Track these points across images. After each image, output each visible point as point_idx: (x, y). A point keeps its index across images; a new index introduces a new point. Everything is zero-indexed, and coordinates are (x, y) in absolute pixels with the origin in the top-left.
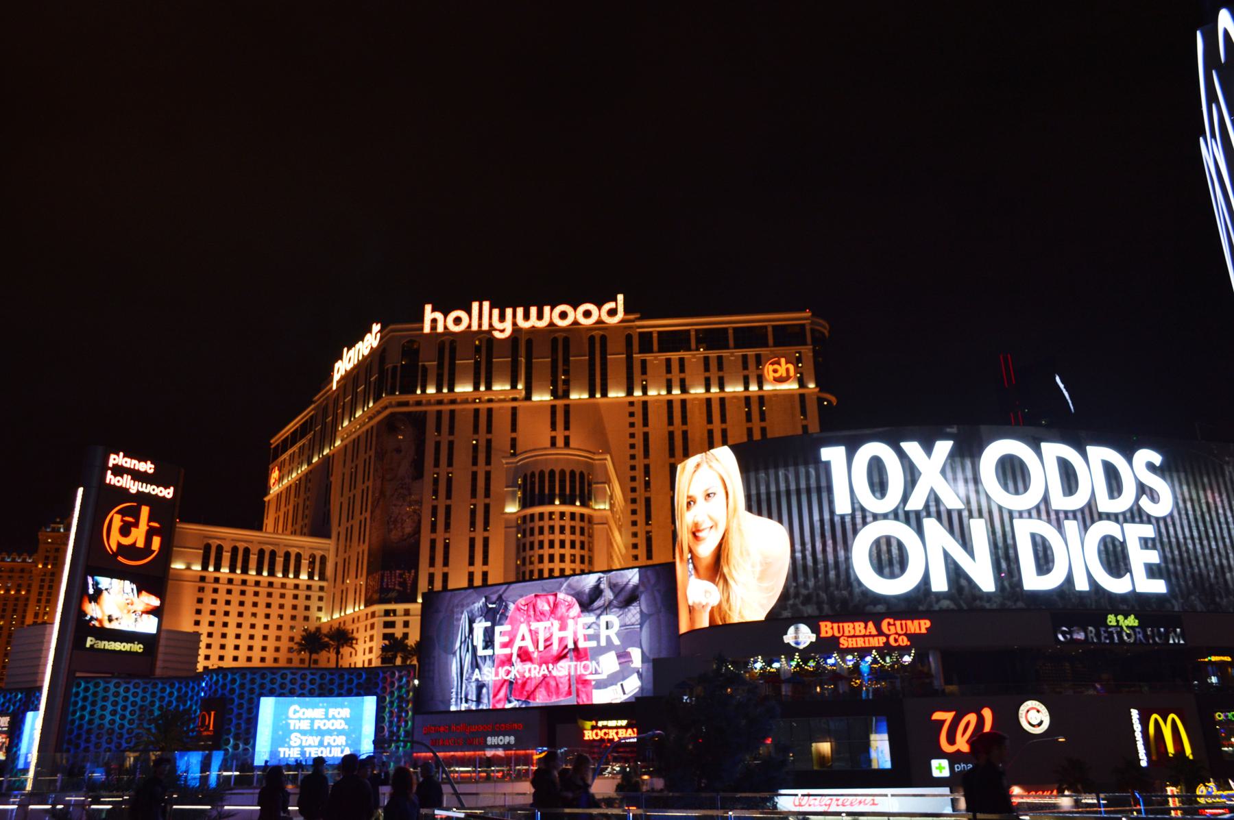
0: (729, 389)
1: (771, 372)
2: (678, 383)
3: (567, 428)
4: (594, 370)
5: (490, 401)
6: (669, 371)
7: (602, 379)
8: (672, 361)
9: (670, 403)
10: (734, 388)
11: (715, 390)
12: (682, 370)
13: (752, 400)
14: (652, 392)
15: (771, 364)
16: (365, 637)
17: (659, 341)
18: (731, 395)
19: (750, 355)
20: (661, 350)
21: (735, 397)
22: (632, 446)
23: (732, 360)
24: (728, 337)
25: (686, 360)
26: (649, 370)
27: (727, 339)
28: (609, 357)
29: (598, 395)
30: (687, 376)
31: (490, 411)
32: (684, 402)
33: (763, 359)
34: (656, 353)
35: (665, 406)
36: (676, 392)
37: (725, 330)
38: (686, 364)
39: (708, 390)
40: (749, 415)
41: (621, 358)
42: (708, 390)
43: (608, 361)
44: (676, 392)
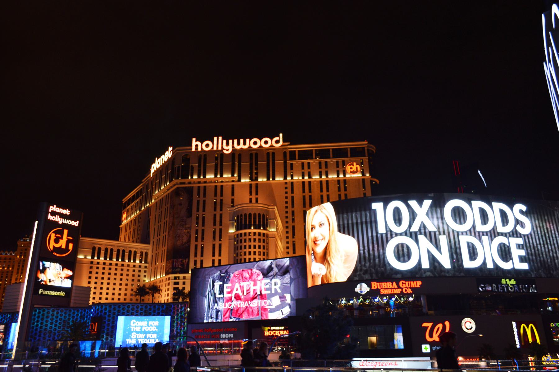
0: (330, 176)
1: (349, 169)
2: (307, 174)
3: (257, 194)
4: (269, 168)
5: (222, 182)
6: (303, 168)
7: (272, 172)
8: (304, 164)
9: (303, 183)
10: (333, 176)
11: (324, 177)
12: (309, 168)
13: (341, 182)
14: (295, 178)
15: (349, 165)
16: (165, 289)
17: (298, 155)
18: (331, 179)
19: (340, 161)
20: (299, 159)
21: (333, 180)
22: (286, 202)
23: (332, 163)
24: (330, 153)
25: (311, 163)
26: (294, 168)
27: (329, 154)
28: (276, 162)
29: (271, 179)
30: (311, 171)
31: (222, 186)
32: (310, 182)
33: (346, 163)
34: (297, 160)
35: (301, 184)
36: (306, 178)
37: (329, 150)
38: (311, 165)
39: (321, 177)
40: (339, 188)
41: (281, 163)
42: (321, 177)
43: (276, 164)
44: (306, 178)
